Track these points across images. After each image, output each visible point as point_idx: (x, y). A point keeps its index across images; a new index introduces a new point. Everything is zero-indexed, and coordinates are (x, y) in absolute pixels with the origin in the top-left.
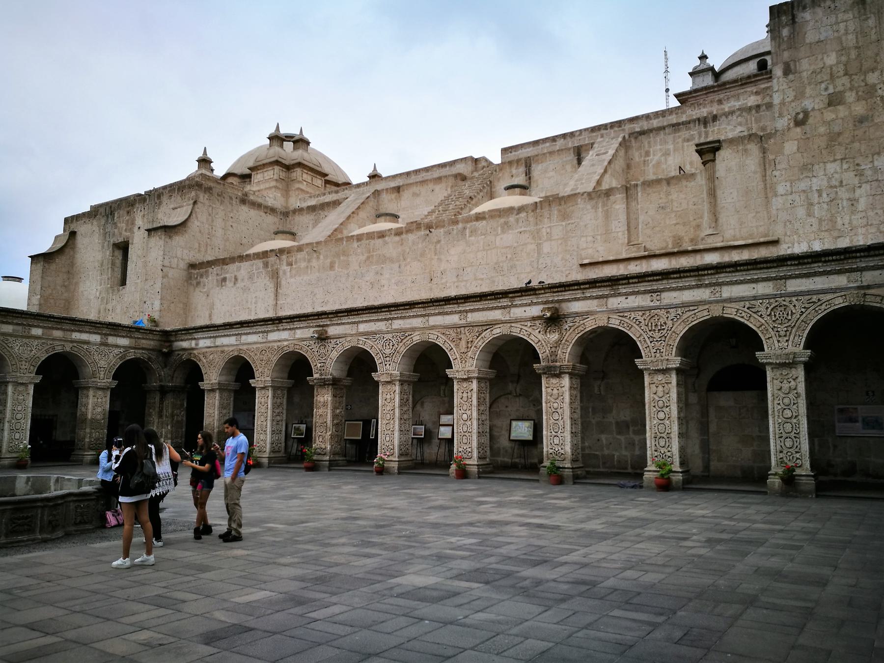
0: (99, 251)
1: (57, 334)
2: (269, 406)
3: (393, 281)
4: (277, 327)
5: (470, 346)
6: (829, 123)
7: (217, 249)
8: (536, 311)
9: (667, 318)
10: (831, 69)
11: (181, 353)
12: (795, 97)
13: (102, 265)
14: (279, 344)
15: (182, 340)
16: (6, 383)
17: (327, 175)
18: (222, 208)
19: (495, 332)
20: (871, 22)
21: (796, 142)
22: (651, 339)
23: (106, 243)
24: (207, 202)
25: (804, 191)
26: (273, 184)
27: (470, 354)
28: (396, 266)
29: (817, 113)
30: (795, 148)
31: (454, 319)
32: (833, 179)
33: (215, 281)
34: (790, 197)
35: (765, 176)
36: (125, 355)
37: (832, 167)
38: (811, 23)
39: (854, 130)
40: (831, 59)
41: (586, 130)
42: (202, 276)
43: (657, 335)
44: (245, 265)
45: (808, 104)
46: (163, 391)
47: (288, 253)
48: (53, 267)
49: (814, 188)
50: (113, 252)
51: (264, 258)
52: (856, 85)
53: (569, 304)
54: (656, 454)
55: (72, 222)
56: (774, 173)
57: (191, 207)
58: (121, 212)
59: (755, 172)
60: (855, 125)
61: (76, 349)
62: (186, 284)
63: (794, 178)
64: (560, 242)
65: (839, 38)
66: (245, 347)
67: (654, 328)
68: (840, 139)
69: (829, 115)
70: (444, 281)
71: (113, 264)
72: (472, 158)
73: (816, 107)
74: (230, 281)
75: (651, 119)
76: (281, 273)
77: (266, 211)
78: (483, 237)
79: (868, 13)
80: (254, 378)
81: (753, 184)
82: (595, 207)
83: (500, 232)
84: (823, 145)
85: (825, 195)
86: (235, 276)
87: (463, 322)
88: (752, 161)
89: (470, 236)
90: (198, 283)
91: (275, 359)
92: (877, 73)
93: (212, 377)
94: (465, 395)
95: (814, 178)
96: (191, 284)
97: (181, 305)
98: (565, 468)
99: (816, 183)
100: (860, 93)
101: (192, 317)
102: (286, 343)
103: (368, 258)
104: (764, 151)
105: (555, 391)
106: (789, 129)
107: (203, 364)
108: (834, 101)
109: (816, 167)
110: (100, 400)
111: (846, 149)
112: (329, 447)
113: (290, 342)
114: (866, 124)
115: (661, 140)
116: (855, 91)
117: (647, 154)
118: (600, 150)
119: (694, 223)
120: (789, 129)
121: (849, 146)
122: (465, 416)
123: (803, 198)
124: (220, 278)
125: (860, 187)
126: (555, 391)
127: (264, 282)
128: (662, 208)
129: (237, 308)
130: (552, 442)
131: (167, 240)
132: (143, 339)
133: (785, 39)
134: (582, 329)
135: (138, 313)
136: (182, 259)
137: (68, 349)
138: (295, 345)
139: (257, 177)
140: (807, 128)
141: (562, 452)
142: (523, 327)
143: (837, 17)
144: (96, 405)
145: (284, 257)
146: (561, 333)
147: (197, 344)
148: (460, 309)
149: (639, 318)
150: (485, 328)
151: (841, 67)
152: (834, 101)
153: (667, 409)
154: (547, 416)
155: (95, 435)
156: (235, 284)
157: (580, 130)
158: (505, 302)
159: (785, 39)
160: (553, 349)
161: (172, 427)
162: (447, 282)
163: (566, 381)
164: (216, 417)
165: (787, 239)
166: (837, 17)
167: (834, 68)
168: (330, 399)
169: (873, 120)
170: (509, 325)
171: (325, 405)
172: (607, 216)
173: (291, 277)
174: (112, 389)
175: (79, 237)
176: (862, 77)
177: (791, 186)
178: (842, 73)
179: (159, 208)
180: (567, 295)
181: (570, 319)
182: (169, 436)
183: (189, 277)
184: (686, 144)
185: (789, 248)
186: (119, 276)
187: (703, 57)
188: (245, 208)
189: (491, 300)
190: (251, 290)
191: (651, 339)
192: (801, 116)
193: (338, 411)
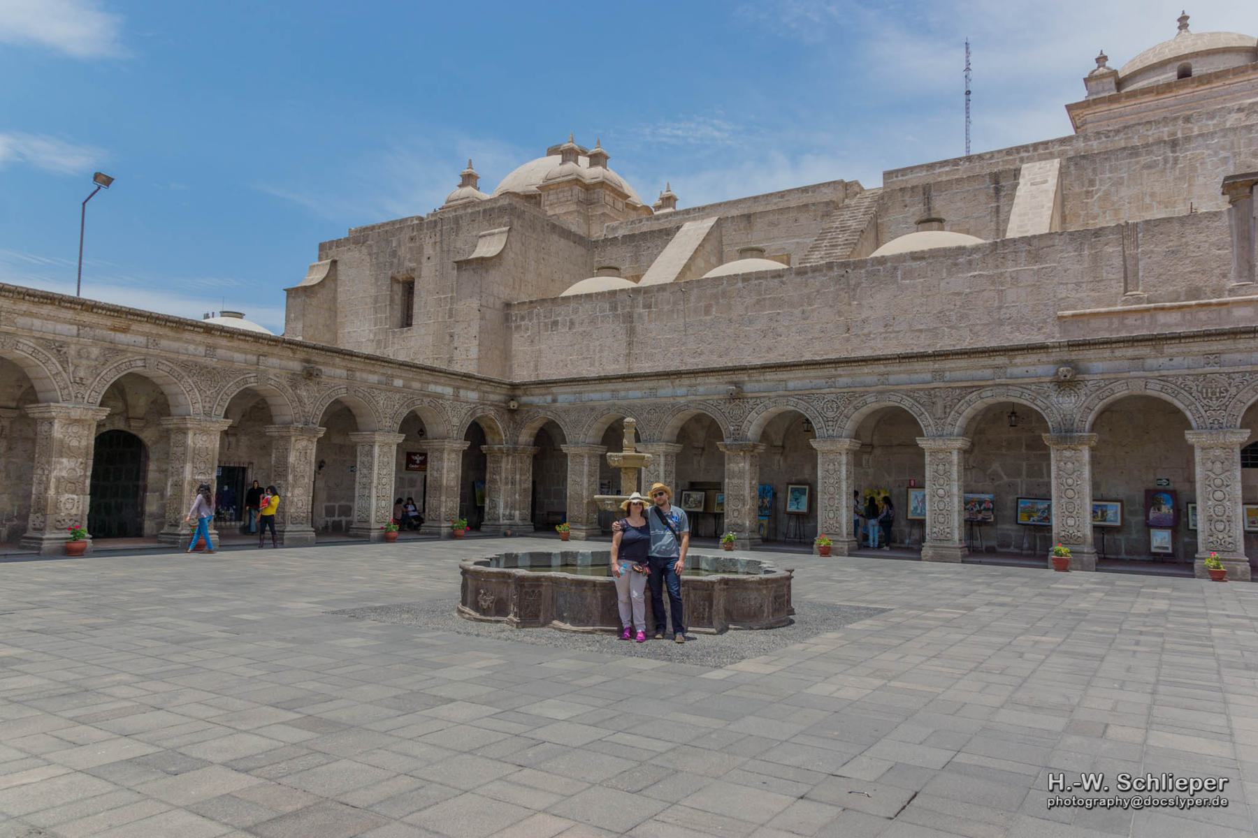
3: (794, 329)
5: (948, 410)
9: (1230, 384)
13: (376, 301)
15: (532, 395)
17: (629, 197)
18: (534, 236)
22: (1206, 408)
27: (949, 420)
28: (797, 312)
41: (999, 152)
43: (1214, 403)
47: (644, 293)
48: (314, 301)
54: (1211, 539)
55: (330, 248)
64: (1029, 289)
67: (1210, 395)
70: (866, 331)
71: (392, 301)
72: (842, 181)
75: (1090, 140)
76: (635, 316)
78: (922, 280)
82: (1079, 249)
83: (945, 275)
86: (571, 319)
89: (903, 279)
94: (941, 467)
98: (1084, 553)
103: (758, 302)
112: (747, 523)
115: (1111, 166)
117: (1092, 183)
118: (1035, 179)
119: (1217, 271)
124: (549, 321)
128: (1173, 252)
130: (1064, 523)
136: (499, 298)
141: (1079, 534)
142: (1026, 391)
145: (640, 299)
149: (1188, 383)
150: (969, 390)
153: (1228, 489)
155: (450, 504)
156: (570, 329)
157: (992, 152)
161: (520, 495)
162: (870, 333)
164: (585, 485)
168: (747, 467)
171: (741, 474)
172: (1096, 259)
173: (650, 322)
174: (464, 451)
175: (340, 267)
182: (517, 506)
184: (1145, 172)
186: (399, 315)
187: (1101, 60)
188: (555, 237)
190: (594, 336)
191: (1206, 408)
193: (754, 482)
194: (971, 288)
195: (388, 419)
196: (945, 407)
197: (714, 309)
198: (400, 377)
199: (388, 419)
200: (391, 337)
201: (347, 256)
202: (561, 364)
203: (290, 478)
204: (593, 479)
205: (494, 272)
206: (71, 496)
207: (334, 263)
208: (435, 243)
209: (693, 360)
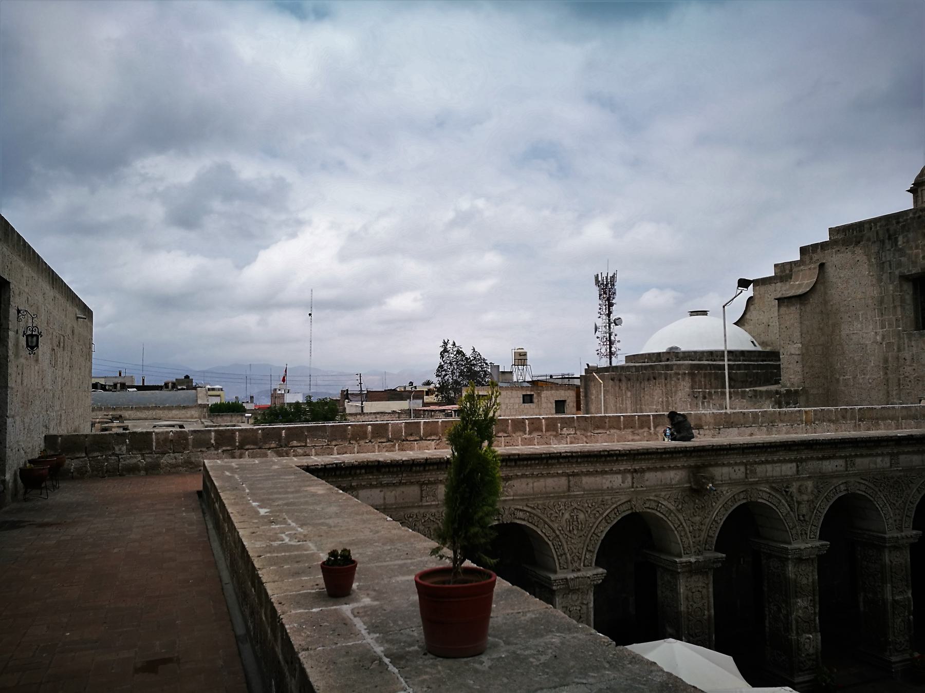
0: (873, 285)
23: (885, 277)
50: (901, 286)
58: (911, 235)
71: (903, 301)
186: (912, 315)
200: (906, 341)
201: (834, 259)
206: (807, 636)
207: (822, 266)
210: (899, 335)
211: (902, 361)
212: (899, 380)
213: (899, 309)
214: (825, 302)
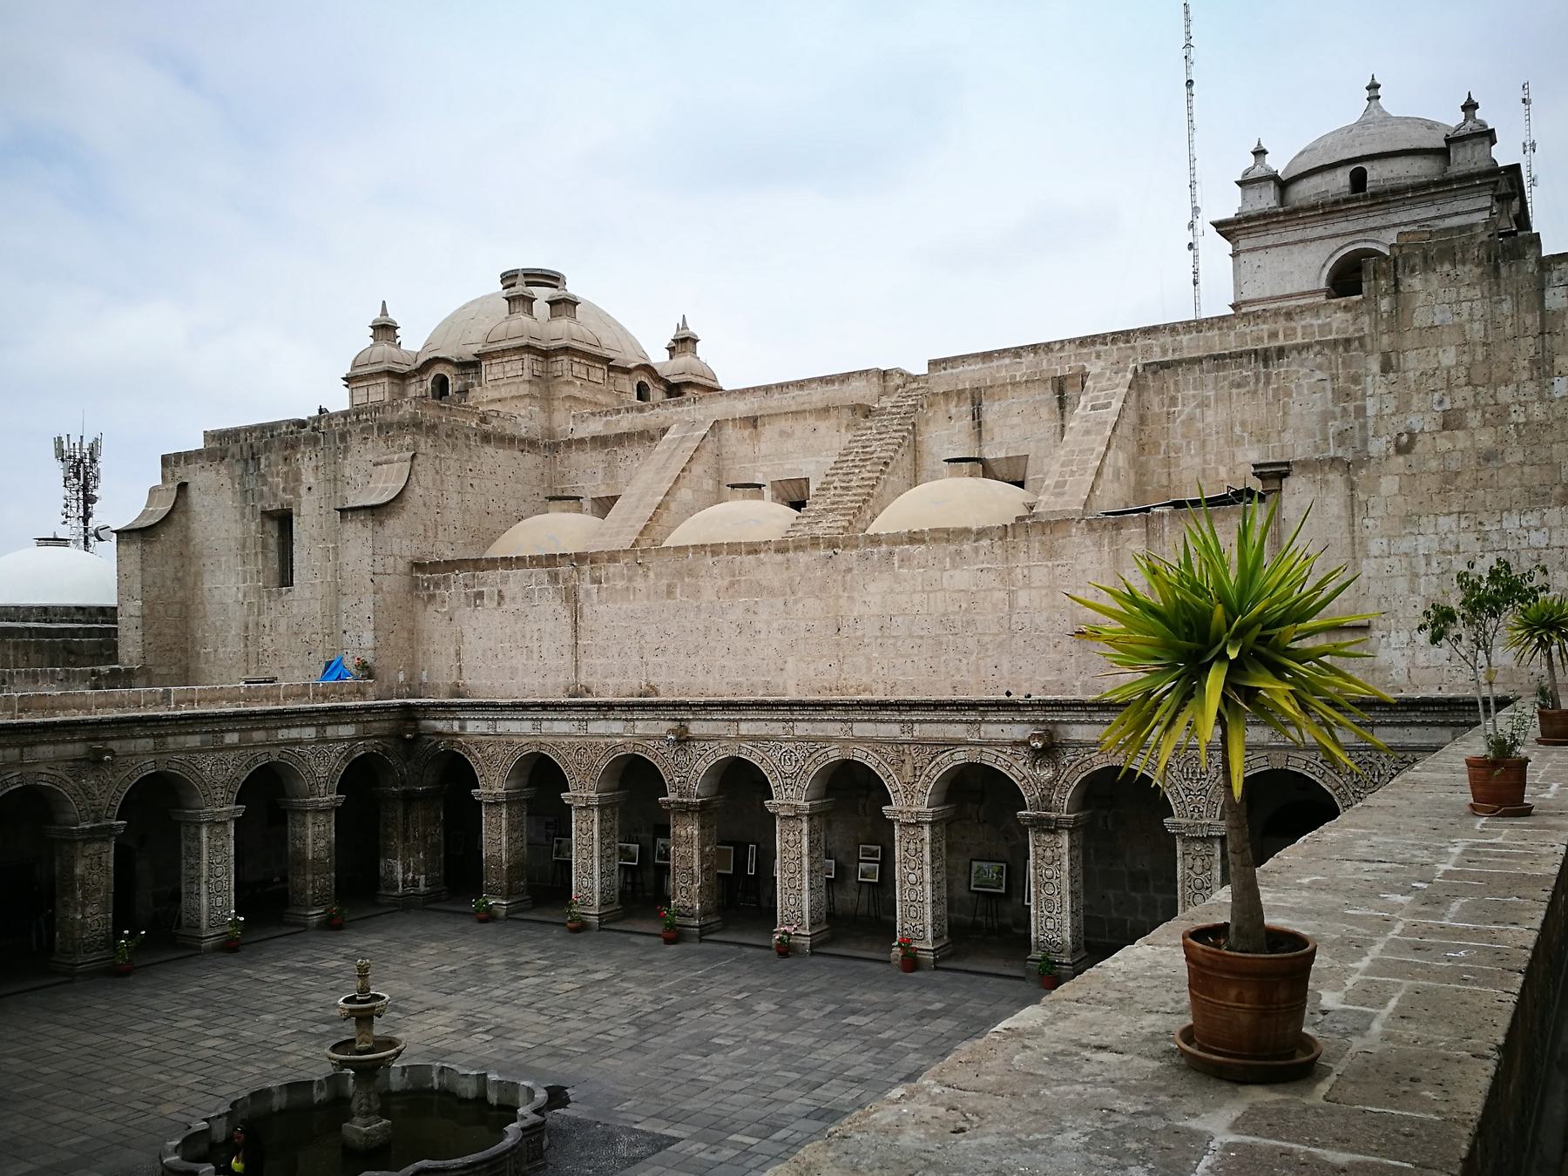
1: (259, 736)
2: (596, 836)
4: (604, 715)
6: (1443, 456)
7: (452, 528)
8: (1018, 732)
10: (1449, 372)
11: (436, 739)
12: (1397, 407)
14: (609, 740)
15: (435, 719)
16: (198, 825)
19: (956, 756)
20: (1506, 307)
21: (1397, 478)
24: (430, 451)
25: (1406, 554)
26: (524, 389)
29: (1427, 438)
30: (1397, 487)
31: (893, 730)
32: (1447, 542)
33: (463, 595)
34: (1387, 561)
35: (1353, 525)
36: (352, 752)
37: (1445, 523)
38: (1422, 296)
39: (1477, 470)
40: (1448, 358)
42: (437, 585)
44: (516, 574)
45: (1415, 422)
46: (409, 798)
49: (1421, 552)
51: (549, 566)
52: (1482, 402)
53: (1069, 728)
56: (1366, 521)
57: (408, 464)
59: (1339, 518)
60: (1479, 464)
61: (285, 756)
62: (409, 597)
63: (1392, 533)
65: (1461, 326)
66: (549, 740)
68: (1458, 482)
69: (1443, 444)
73: (1426, 429)
74: (491, 599)
77: (522, 447)
79: (1503, 292)
80: (568, 791)
81: (1335, 535)
84: (1434, 488)
85: (1434, 564)
86: (500, 591)
87: (906, 737)
88: (1334, 501)
90: (432, 597)
91: (603, 764)
92: (1512, 387)
93: (493, 783)
94: (912, 846)
95: (1420, 537)
96: (418, 596)
97: (405, 635)
99: (1424, 544)
100: (1487, 415)
101: (424, 653)
102: (619, 741)
104: (1352, 486)
105: (1048, 853)
106: (1388, 457)
107: (476, 760)
108: (1451, 422)
109: (1424, 520)
110: (322, 828)
111: (1466, 498)
113: (626, 739)
114: (1494, 463)
116: (1480, 411)
120: (1388, 457)
121: (1470, 495)
122: (912, 878)
123: (1404, 564)
125: (1482, 557)
126: (1048, 853)
127: (550, 606)
129: (507, 645)
130: (1043, 925)
131: (377, 528)
132: (375, 721)
133: (1385, 315)
134: (1088, 767)
135: (321, 636)
137: (275, 758)
138: (635, 744)
139: (491, 371)
140: (1412, 458)
142: (1000, 755)
143: (1458, 293)
144: (317, 837)
146: (1057, 770)
147: (462, 728)
148: (903, 717)
151: (1462, 371)
152: (1451, 422)
154: (1036, 887)
155: (320, 882)
156: (499, 604)
158: (972, 715)
159: (1385, 315)
160: (1045, 792)
163: (1064, 840)
165: (1381, 624)
166: (1458, 293)
167: (1453, 372)
168: (696, 832)
169: (1503, 459)
170: (979, 749)
171: (689, 841)
174: (338, 810)
176: (1491, 392)
177: (1389, 545)
178: (1462, 381)
179: (345, 458)
180: (1066, 716)
181: (1071, 750)
183: (415, 585)
185: (1383, 637)
188: (489, 449)
189: (950, 710)
190: (530, 617)
192: (1405, 439)
194: (977, 586)
195: (219, 790)
196: (915, 768)
197: (678, 591)
198: (234, 730)
199: (219, 790)
200: (266, 600)
202: (489, 654)
203: (79, 894)
204: (515, 835)
205: (391, 522)
208: (317, 467)
209: (655, 659)
210: (259, 592)
211: (261, 628)
212: (258, 654)
213: (260, 557)
214: (186, 541)
